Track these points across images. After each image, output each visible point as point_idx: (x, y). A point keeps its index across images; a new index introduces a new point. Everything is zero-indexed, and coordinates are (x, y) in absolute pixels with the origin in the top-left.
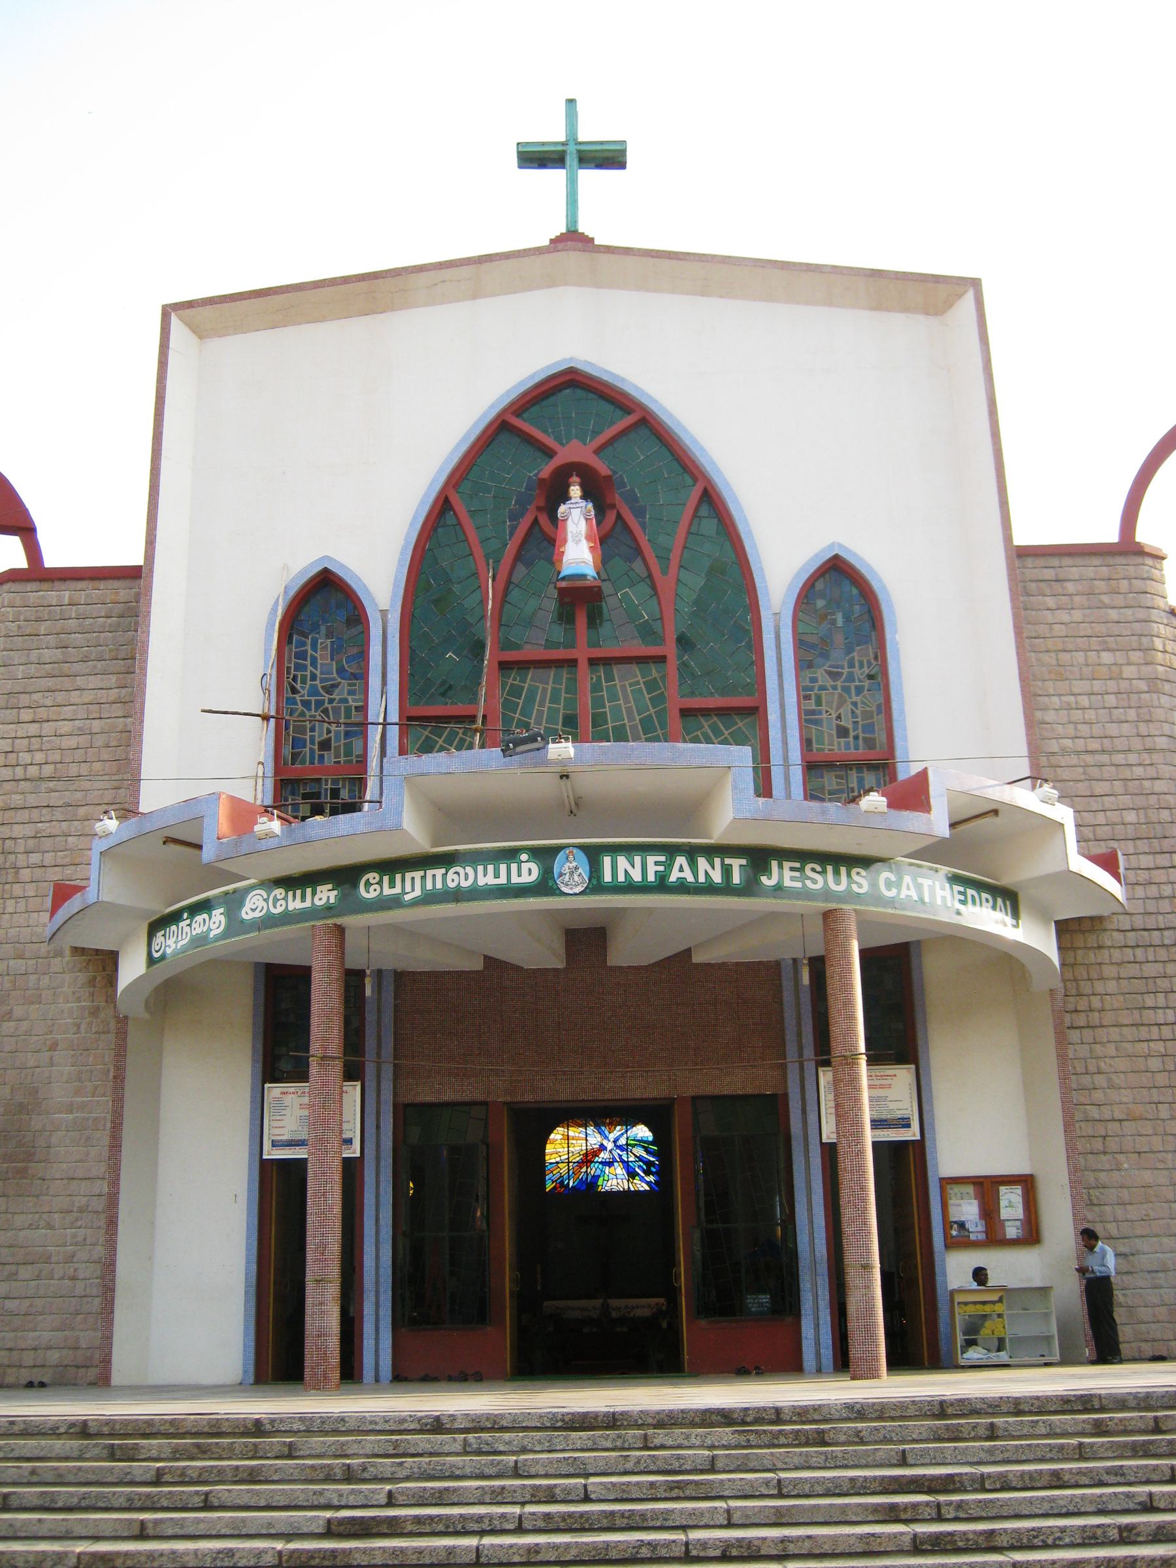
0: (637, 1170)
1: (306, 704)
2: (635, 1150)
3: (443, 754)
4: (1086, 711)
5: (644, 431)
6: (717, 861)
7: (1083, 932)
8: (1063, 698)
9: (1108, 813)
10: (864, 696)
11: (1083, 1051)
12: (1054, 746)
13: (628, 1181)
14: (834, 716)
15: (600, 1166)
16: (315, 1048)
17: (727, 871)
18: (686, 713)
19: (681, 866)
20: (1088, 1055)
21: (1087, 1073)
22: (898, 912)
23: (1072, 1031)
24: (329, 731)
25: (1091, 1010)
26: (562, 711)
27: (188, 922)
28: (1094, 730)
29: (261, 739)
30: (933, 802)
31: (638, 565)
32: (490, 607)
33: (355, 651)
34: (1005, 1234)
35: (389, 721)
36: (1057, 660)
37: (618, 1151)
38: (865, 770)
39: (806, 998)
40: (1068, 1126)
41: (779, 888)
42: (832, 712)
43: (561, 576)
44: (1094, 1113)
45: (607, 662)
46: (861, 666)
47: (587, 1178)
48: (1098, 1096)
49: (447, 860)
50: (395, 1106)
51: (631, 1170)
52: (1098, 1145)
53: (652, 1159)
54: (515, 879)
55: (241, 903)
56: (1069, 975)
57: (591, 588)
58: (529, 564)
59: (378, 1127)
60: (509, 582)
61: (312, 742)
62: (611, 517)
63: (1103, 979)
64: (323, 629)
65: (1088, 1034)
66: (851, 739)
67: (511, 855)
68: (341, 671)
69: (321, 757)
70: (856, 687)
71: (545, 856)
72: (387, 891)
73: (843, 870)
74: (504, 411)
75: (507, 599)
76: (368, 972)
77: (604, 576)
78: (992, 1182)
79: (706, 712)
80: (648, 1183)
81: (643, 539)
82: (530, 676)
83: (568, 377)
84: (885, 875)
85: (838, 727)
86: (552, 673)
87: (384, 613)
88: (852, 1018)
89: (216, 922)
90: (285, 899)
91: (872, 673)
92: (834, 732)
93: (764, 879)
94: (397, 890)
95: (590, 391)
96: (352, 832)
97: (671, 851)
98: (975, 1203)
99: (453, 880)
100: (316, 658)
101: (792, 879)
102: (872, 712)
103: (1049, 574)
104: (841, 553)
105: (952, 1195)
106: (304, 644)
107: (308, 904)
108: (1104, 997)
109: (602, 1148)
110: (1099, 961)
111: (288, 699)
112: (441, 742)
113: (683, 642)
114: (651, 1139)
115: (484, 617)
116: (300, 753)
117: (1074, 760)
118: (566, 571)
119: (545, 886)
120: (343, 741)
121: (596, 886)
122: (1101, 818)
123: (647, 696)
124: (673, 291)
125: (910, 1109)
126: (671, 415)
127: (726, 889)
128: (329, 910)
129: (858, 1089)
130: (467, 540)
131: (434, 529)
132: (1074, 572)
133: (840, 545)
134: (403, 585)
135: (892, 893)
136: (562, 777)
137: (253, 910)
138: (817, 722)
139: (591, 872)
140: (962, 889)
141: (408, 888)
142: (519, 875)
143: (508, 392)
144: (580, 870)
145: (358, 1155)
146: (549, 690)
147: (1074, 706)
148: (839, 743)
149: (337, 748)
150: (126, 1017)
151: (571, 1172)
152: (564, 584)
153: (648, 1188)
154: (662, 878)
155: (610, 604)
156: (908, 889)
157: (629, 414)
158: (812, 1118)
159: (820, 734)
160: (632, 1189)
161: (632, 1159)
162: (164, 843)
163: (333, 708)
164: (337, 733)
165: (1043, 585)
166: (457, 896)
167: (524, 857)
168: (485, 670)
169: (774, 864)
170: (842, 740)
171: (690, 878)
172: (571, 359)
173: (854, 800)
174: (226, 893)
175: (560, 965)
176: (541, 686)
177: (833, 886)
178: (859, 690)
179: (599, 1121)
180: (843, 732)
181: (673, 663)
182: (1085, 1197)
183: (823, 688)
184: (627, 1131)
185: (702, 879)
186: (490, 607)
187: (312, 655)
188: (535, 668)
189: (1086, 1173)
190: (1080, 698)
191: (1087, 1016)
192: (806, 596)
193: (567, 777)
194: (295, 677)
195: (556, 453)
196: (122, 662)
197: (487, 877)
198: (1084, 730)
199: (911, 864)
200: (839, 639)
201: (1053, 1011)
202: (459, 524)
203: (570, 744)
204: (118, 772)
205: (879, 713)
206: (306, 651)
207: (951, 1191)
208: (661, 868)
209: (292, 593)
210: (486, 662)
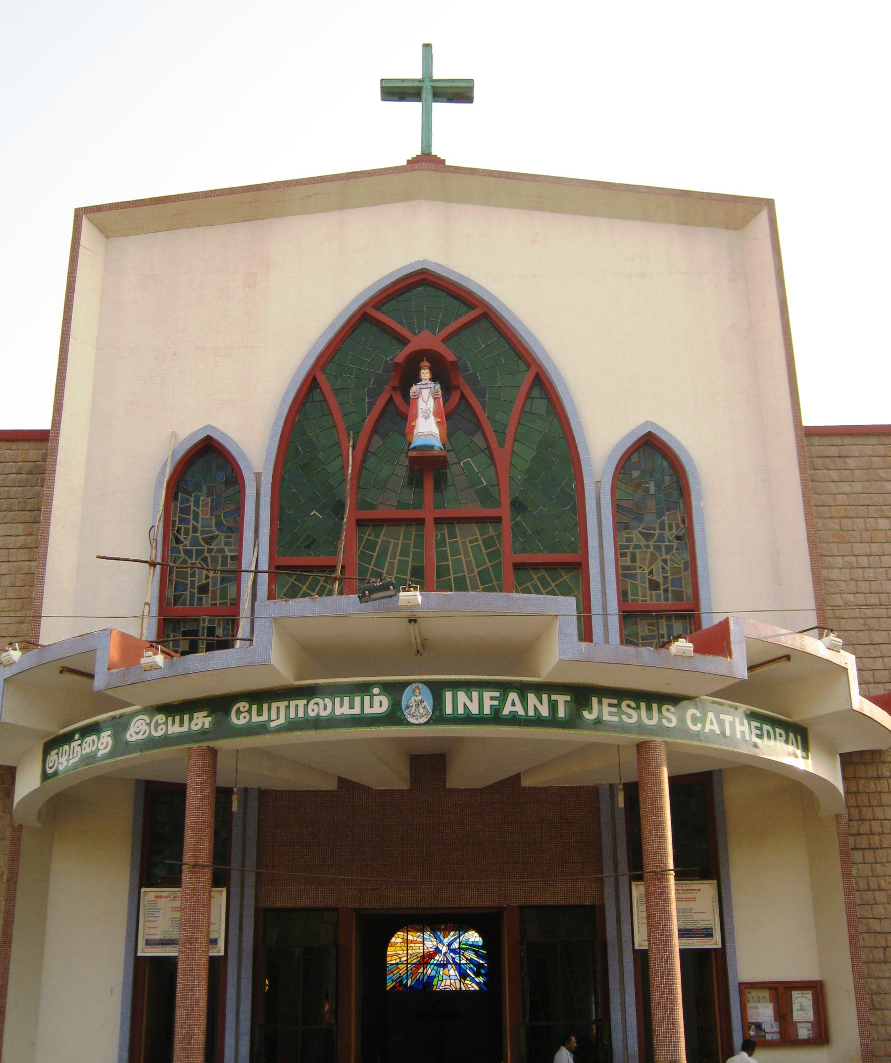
0: (468, 971)
1: (188, 553)
2: (466, 954)
3: (307, 599)
4: (866, 570)
5: (485, 324)
6: (545, 697)
7: (864, 764)
8: (845, 558)
9: (885, 659)
10: (673, 555)
11: (866, 869)
12: (838, 600)
13: (460, 981)
14: (647, 571)
15: (436, 968)
16: (188, 857)
17: (553, 706)
18: (518, 567)
19: (513, 701)
20: (870, 874)
21: (869, 890)
22: (703, 744)
23: (855, 852)
24: (207, 577)
25: (872, 833)
26: (410, 564)
27: (79, 742)
28: (872, 587)
29: (148, 583)
30: (734, 647)
31: (478, 439)
32: (350, 472)
33: (231, 507)
34: (797, 1035)
35: (260, 569)
36: (840, 525)
37: (451, 954)
38: (673, 618)
39: (621, 819)
40: (853, 937)
41: (598, 722)
42: (646, 569)
43: (412, 446)
44: (875, 925)
45: (451, 521)
46: (671, 529)
47: (423, 978)
48: (879, 910)
49: (308, 692)
50: (257, 910)
51: (462, 971)
52: (879, 954)
53: (481, 962)
54: (368, 710)
55: (126, 727)
56: (853, 802)
57: (436, 458)
58: (384, 436)
59: (241, 929)
60: (366, 451)
61: (193, 587)
62: (456, 396)
63: (882, 805)
64: (205, 488)
65: (869, 855)
66: (662, 591)
67: (364, 689)
68: (219, 525)
69: (200, 599)
70: (666, 547)
71: (394, 690)
72: (255, 719)
73: (655, 706)
74: (365, 305)
75: (365, 465)
76: (235, 790)
77: (449, 447)
78: (785, 987)
79: (536, 566)
80: (478, 984)
81: (483, 416)
82: (383, 532)
83: (422, 277)
84: (692, 712)
85: (650, 581)
86: (402, 530)
87: (258, 476)
88: (662, 838)
89: (103, 743)
90: (166, 723)
91: (680, 534)
92: (647, 586)
93: (585, 714)
94: (264, 718)
95: (439, 289)
96: (226, 666)
97: (505, 687)
98: (771, 1006)
99: (313, 710)
100: (198, 513)
101: (610, 714)
102: (679, 568)
103: (833, 451)
104: (654, 431)
105: (751, 999)
106: (188, 501)
107: (185, 728)
108: (883, 822)
110: (879, 790)
111: (172, 548)
112: (304, 588)
113: (517, 505)
114: (481, 943)
115: (344, 480)
116: (183, 595)
117: (856, 613)
118: (416, 442)
119: (394, 717)
120: (219, 586)
121: (438, 717)
122: (879, 664)
123: (484, 552)
124: (512, 205)
125: (713, 920)
126: (509, 310)
127: (553, 722)
128: (203, 734)
129: (667, 902)
130: (331, 414)
131: (303, 404)
132: (855, 450)
133: (653, 424)
134: (275, 452)
135: (698, 727)
136: (410, 621)
137: (137, 733)
138: (632, 577)
139: (434, 705)
140: (758, 725)
141: (274, 716)
142: (372, 707)
143: (369, 288)
144: (425, 703)
145: (222, 953)
146: (400, 545)
147: (855, 565)
148: (651, 595)
149: (214, 592)
150: (21, 826)
151: (409, 973)
152: (414, 454)
153: (477, 988)
154: (496, 711)
155: (454, 471)
156: (712, 724)
157: (473, 309)
158: (626, 927)
159: (635, 588)
160: (463, 989)
162: (61, 672)
163: (210, 556)
164: (215, 578)
165: (828, 460)
166: (317, 724)
167: (376, 691)
168: (345, 527)
169: (595, 700)
170: (654, 592)
171: (521, 712)
172: (424, 261)
173: (665, 645)
174: (114, 718)
175: (405, 786)
176: (392, 541)
177: (646, 721)
178: (669, 549)
180: (654, 586)
181: (507, 522)
182: (869, 1002)
183: (637, 547)
184: (459, 937)
185: (531, 713)
186: (350, 472)
187: (194, 510)
188: (388, 525)
189: (869, 980)
190: (860, 558)
191: (869, 839)
192: (623, 467)
193: (415, 621)
194: (179, 531)
195: (409, 341)
196: (29, 513)
197: (343, 708)
198: (864, 586)
199: (714, 702)
200: (651, 504)
201: (838, 834)
202: (325, 400)
203: (418, 593)
204: (22, 608)
205: (686, 569)
206: (190, 506)
207: (749, 995)
208: (496, 703)
209: (178, 457)
210: (345, 520)
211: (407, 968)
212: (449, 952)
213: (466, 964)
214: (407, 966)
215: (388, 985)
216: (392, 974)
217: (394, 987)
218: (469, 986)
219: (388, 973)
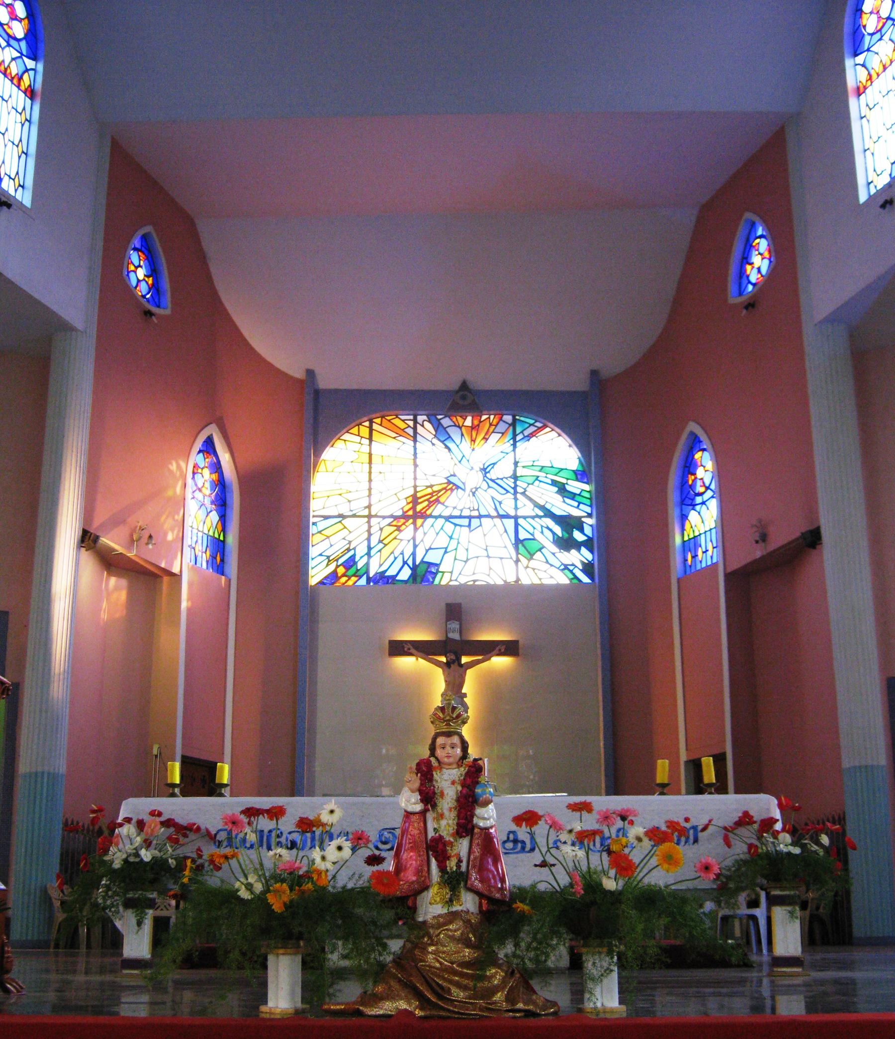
0: (538, 535)
15: (449, 527)
47: (414, 554)
51: (523, 535)
53: (576, 513)
109: (451, 486)
151: (374, 540)
153: (563, 579)
160: (526, 580)
161: (527, 509)
179: (446, 422)
211: (370, 527)
212: (485, 485)
213: (533, 517)
214: (369, 522)
215: (311, 572)
216: (326, 543)
217: (334, 576)
218: (541, 575)
219: (314, 540)
